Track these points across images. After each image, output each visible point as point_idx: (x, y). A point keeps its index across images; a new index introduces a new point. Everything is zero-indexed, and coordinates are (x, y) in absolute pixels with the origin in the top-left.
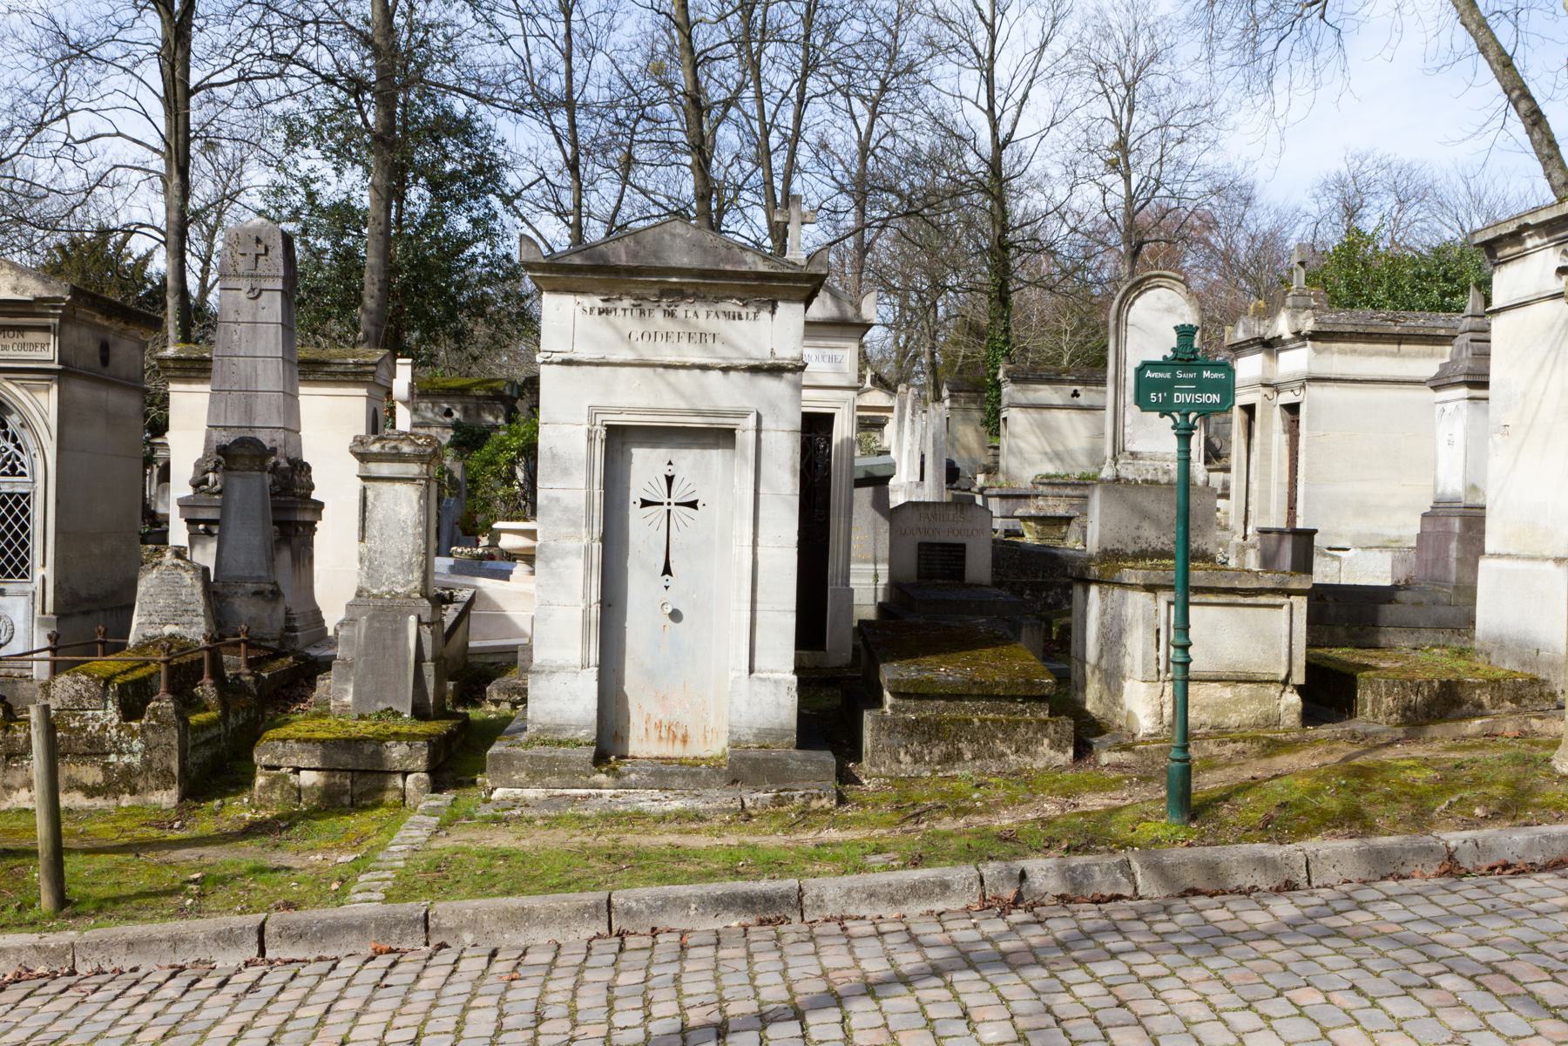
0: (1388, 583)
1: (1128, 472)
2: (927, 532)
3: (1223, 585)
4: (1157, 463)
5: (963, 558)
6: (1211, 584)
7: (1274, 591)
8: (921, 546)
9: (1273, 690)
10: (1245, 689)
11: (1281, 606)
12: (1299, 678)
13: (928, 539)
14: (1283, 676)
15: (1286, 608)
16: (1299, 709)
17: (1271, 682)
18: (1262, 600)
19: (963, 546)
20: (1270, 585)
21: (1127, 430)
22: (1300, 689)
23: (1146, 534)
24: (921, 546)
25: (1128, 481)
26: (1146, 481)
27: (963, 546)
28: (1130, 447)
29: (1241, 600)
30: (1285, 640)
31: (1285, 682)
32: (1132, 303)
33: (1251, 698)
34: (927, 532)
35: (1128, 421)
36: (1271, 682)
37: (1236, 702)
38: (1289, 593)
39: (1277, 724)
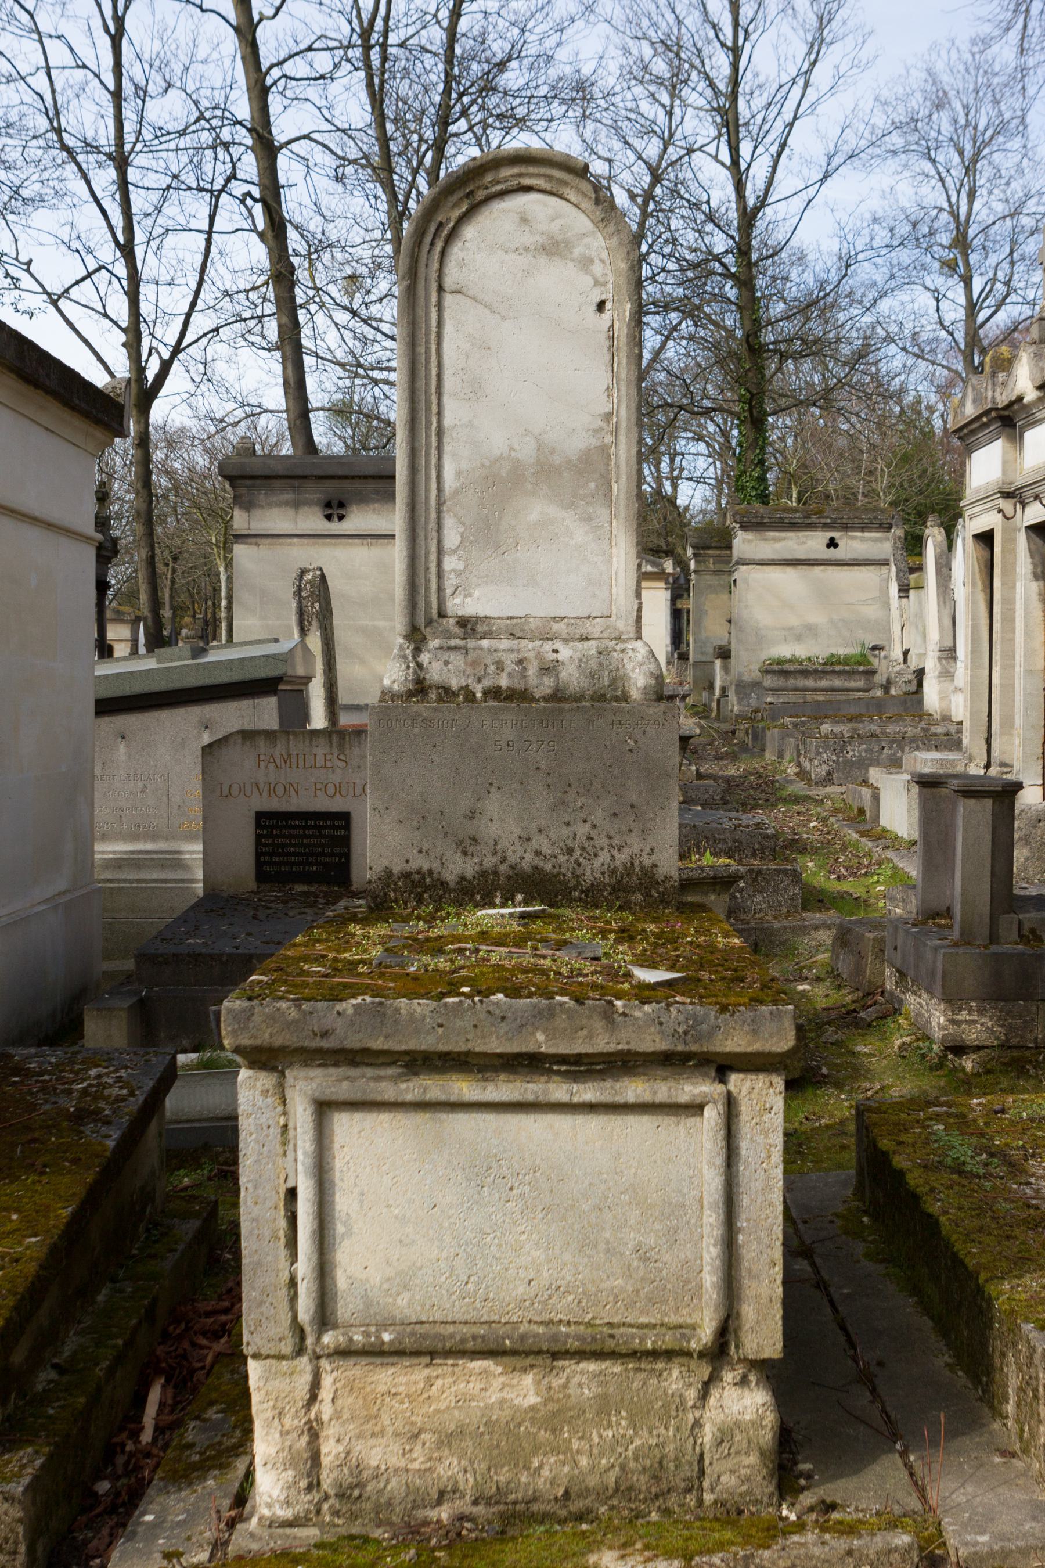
0: (800, 1259)
1: (444, 668)
2: (272, 791)
3: (495, 1045)
4: (528, 647)
5: (346, 841)
6: (459, 1046)
7: (669, 1063)
8: (263, 819)
9: (676, 1380)
10: (582, 1379)
11: (696, 1108)
12: (763, 1334)
13: (274, 804)
14: (706, 1334)
15: (712, 1114)
16: (767, 1437)
17: (669, 1355)
18: (634, 1089)
19: (344, 819)
20: (652, 1042)
21: (450, 563)
22: (767, 1371)
23: (494, 830)
24: (263, 819)
25: (446, 693)
26: (494, 693)
27: (344, 819)
28: (460, 605)
29: (559, 1091)
30: (712, 1221)
31: (720, 1350)
32: (453, 235)
33: (604, 1406)
34: (272, 791)
35: (452, 537)
36: (669, 1355)
37: (556, 1416)
38: (722, 1067)
39: (695, 1484)
